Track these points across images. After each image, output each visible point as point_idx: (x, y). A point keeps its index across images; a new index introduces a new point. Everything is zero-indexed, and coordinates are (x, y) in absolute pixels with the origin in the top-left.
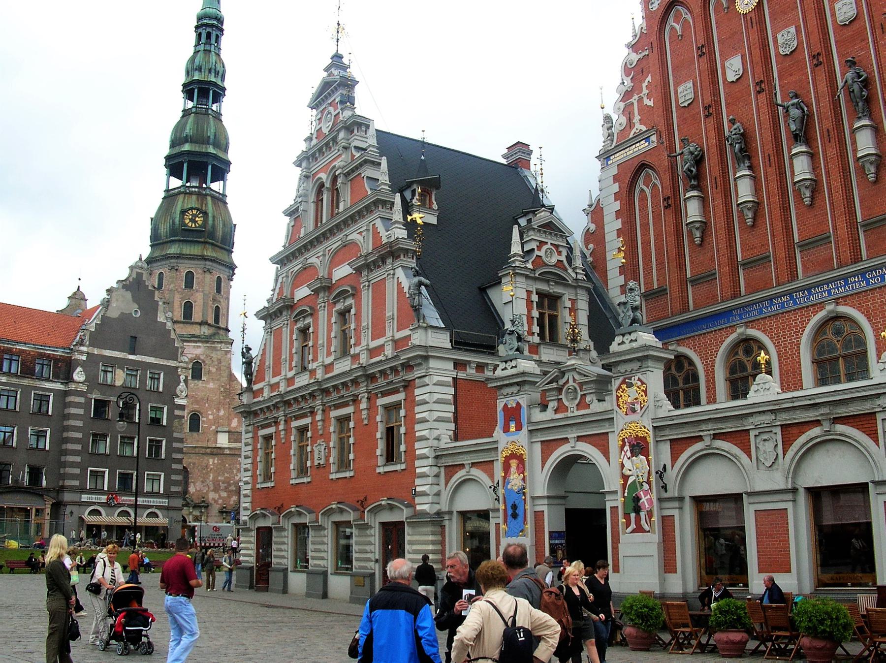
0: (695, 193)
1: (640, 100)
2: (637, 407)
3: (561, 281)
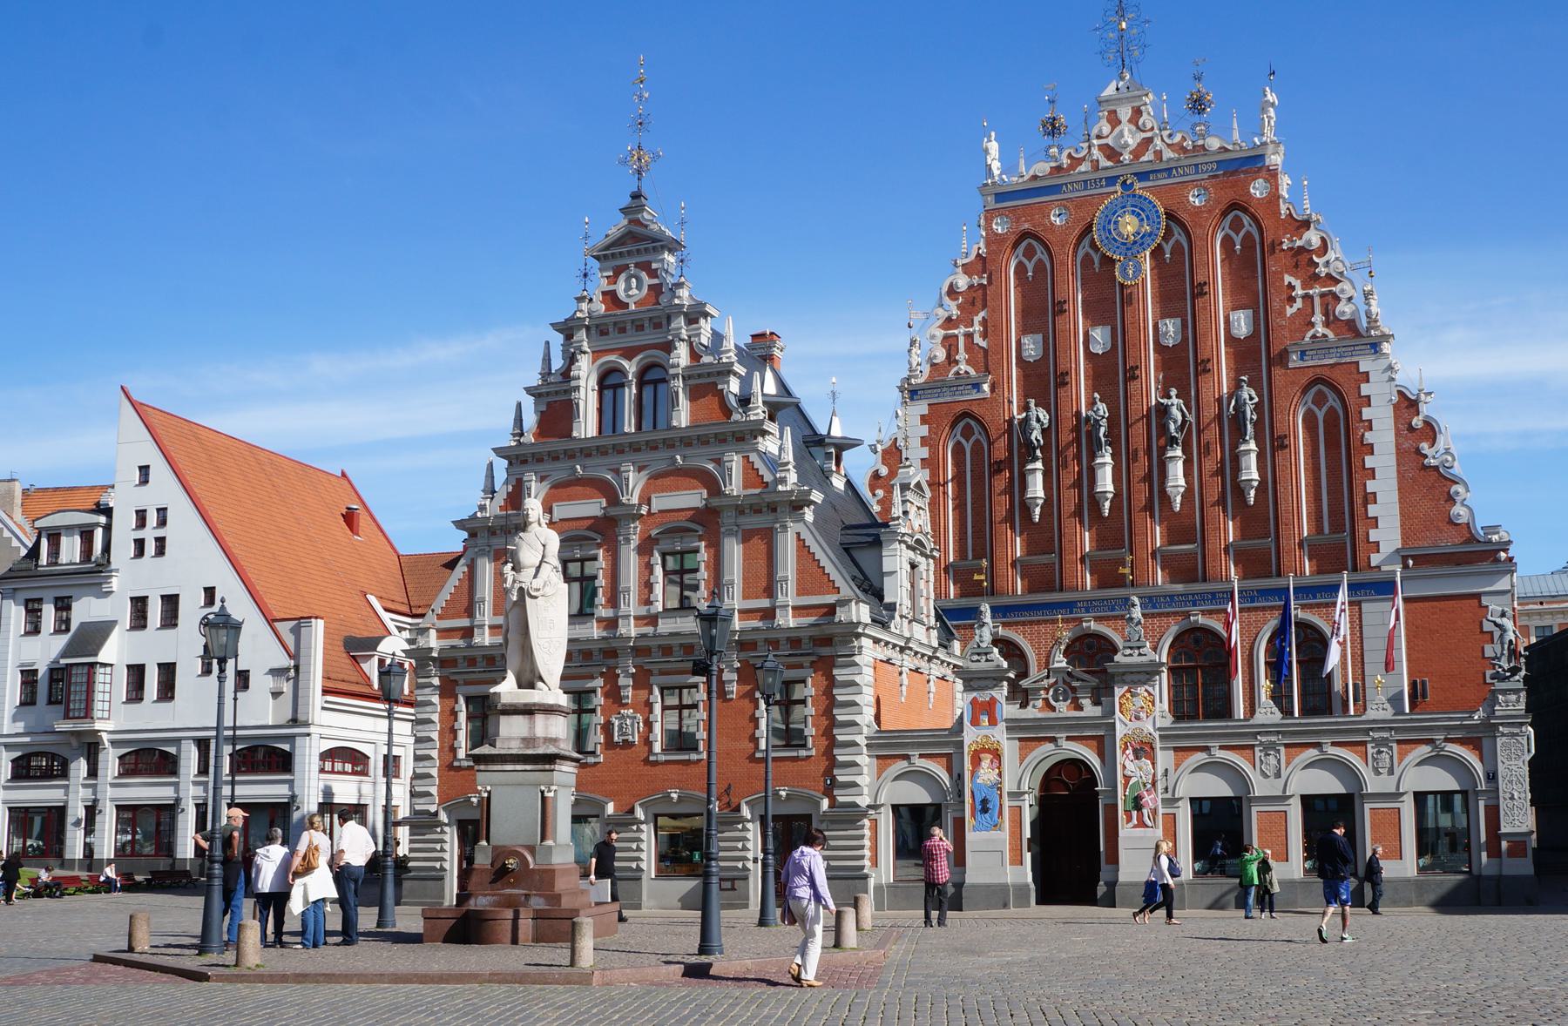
1: (969, 336)
2: (1143, 715)
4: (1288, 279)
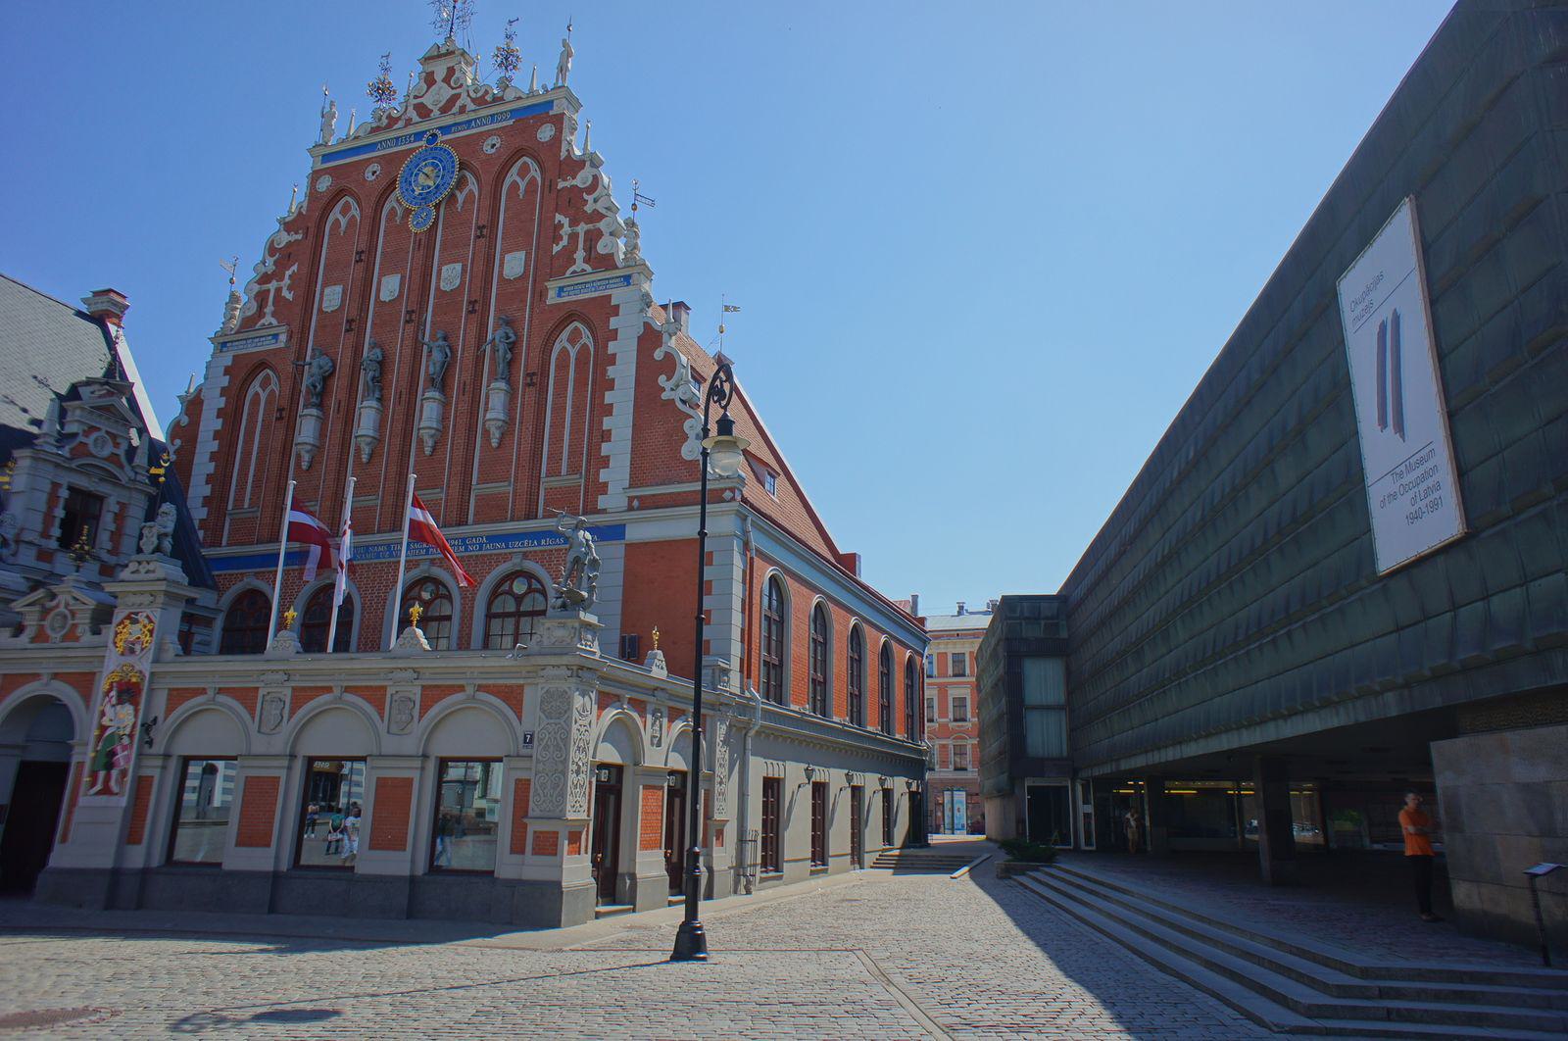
0: (314, 411)
1: (279, 290)
2: (138, 648)
3: (113, 479)
4: (558, 217)
